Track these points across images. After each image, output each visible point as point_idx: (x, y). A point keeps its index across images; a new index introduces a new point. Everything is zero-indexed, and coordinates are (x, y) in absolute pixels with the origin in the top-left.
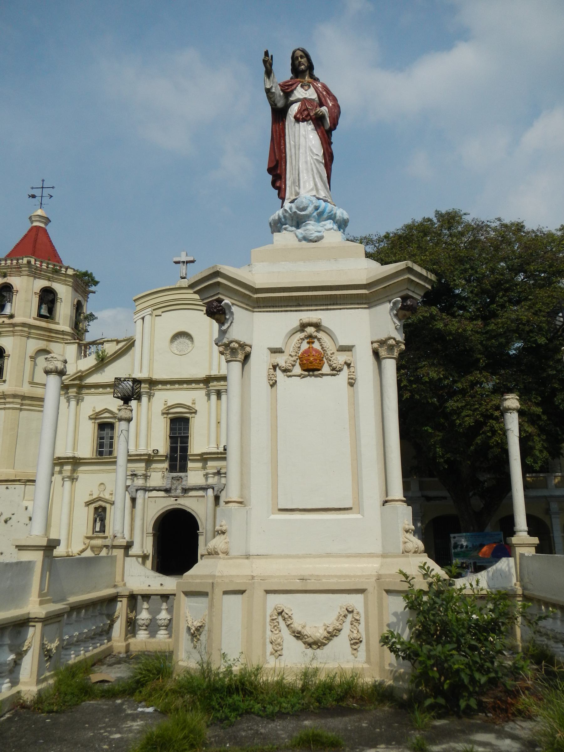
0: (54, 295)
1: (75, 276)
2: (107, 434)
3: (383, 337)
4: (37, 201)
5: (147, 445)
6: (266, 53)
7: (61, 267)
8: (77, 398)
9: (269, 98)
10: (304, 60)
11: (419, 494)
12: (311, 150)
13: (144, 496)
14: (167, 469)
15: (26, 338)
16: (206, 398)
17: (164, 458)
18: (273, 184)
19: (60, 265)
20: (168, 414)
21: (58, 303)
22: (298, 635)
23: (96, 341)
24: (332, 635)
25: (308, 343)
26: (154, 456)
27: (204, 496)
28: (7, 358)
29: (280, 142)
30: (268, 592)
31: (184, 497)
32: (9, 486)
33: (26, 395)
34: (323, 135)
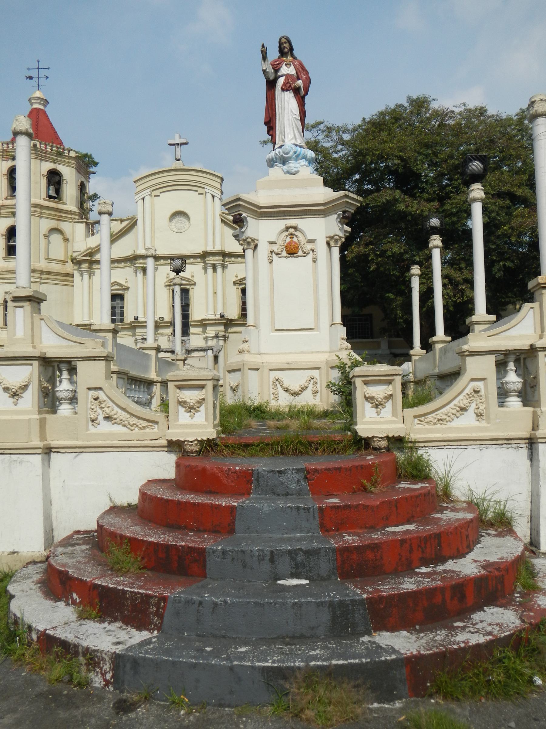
1: (77, 158)
2: (118, 304)
3: (332, 235)
6: (263, 46)
7: (64, 149)
9: (265, 75)
10: (286, 45)
11: (388, 352)
12: (292, 111)
16: (203, 271)
18: (268, 132)
19: (63, 147)
22: (286, 390)
24: (303, 389)
25: (290, 238)
26: (160, 323)
27: (205, 356)
29: (272, 104)
30: (270, 370)
34: (299, 100)
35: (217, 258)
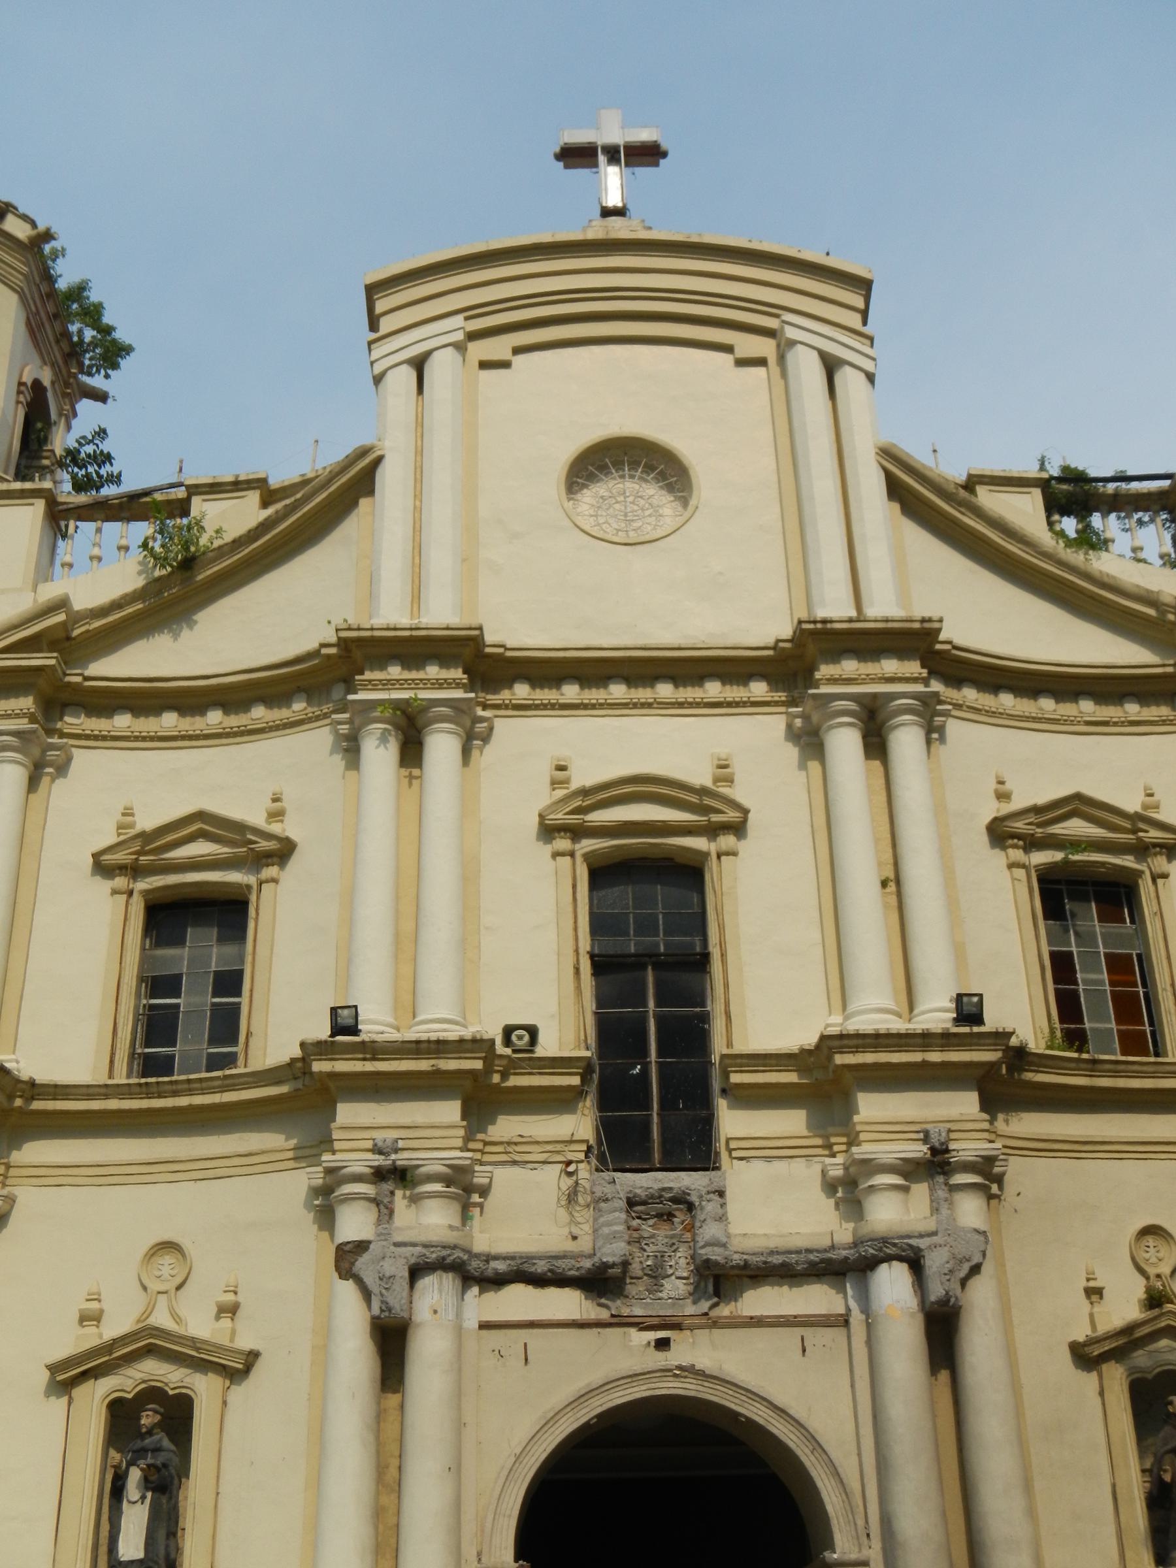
5: (466, 997)
8: (36, 752)
13: (459, 1314)
14: (589, 1148)
17: (575, 1081)
20: (576, 832)
23: (147, 493)
31: (715, 1324)
35: (890, 666)
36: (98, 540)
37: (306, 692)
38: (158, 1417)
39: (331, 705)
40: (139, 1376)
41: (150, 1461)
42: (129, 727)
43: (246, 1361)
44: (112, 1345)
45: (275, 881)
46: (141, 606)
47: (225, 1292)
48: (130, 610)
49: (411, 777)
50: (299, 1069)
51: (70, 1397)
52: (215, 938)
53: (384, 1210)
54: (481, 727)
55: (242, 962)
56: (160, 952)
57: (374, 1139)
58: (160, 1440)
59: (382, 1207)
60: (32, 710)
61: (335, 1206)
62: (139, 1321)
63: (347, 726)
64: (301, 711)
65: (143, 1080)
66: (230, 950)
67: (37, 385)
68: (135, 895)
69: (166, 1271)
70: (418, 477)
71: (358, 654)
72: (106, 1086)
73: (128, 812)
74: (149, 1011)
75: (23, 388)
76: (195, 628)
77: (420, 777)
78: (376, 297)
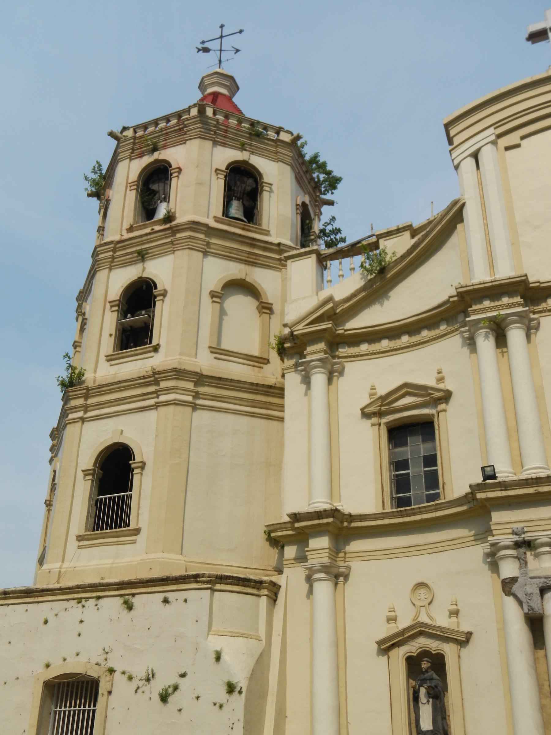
0: (256, 181)
4: (212, 57)
8: (329, 366)
15: (201, 254)
21: (264, 193)
23: (359, 242)
28: (161, 298)
32: (171, 596)
33: (205, 373)
36: (341, 267)
37: (446, 320)
38: (429, 664)
39: (458, 324)
40: (418, 645)
41: (429, 684)
42: (367, 349)
43: (466, 637)
44: (403, 631)
45: (445, 411)
46: (364, 294)
47: (451, 605)
48: (360, 297)
49: (503, 353)
50: (471, 498)
51: (388, 656)
52: (421, 440)
53: (523, 562)
54: (533, 323)
55: (435, 450)
56: (398, 450)
57: (512, 528)
58: (432, 675)
59: (521, 560)
60: (325, 348)
61: (498, 562)
62: (414, 620)
63: (468, 333)
64: (445, 329)
65: (399, 509)
66: (429, 445)
67: (304, 204)
68: (382, 425)
69: (423, 596)
70: (484, 209)
71: (468, 298)
72: (383, 513)
73: (373, 388)
74: (396, 477)
75: (298, 207)
76: (390, 299)
77: (507, 352)
78: (449, 129)
